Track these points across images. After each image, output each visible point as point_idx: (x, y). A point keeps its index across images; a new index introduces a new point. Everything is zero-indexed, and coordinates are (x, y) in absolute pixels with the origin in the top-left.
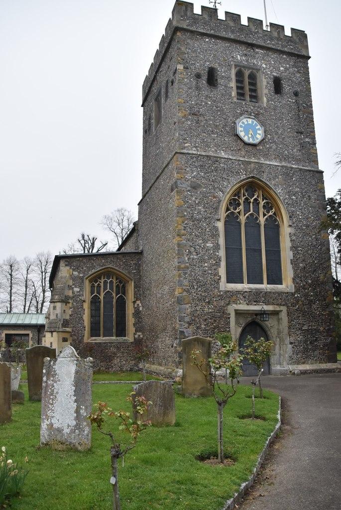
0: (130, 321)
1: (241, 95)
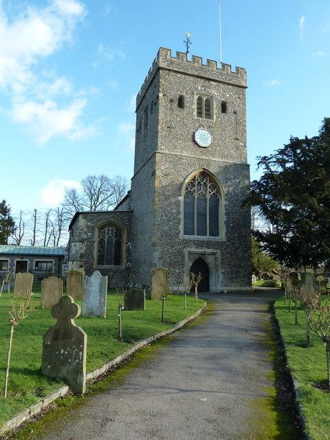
0: (124, 255)
1: (200, 114)
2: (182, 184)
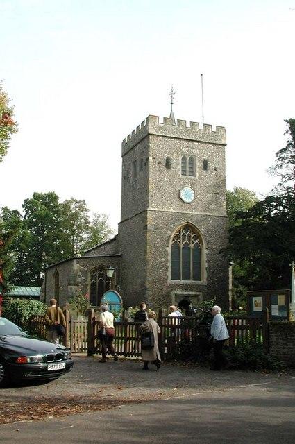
1: (184, 172)
2: (169, 237)
